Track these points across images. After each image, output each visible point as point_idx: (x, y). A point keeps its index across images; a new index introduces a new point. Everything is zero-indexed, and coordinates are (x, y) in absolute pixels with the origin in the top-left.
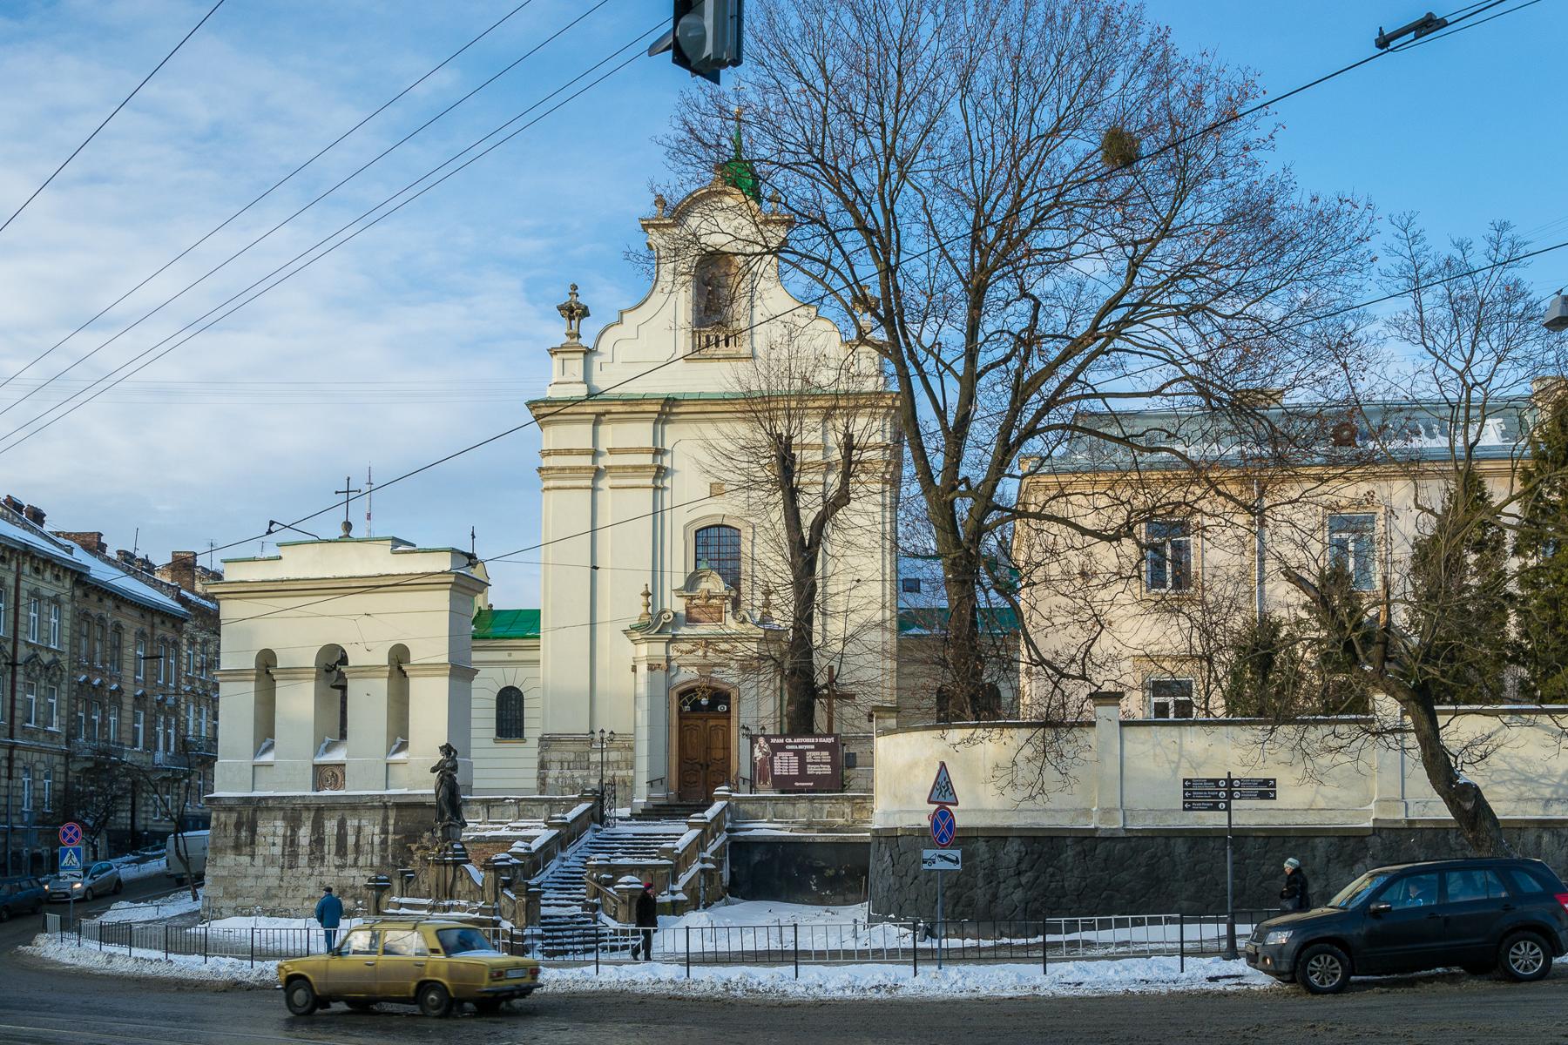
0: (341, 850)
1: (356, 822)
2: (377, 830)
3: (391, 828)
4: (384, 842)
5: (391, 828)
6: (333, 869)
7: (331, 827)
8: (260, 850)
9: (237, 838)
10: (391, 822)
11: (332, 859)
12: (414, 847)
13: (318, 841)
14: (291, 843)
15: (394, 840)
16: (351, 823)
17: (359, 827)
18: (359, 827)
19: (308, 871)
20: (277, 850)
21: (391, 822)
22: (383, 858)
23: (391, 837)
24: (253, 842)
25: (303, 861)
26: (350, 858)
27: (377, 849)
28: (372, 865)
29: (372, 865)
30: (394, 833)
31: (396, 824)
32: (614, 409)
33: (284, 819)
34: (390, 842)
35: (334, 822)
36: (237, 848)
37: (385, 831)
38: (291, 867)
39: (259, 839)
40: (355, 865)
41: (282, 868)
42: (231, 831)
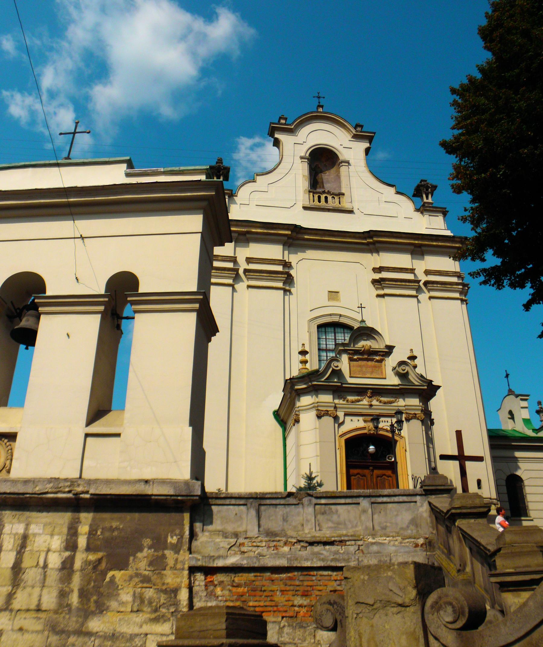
1: (20, 529)
2: (57, 542)
3: (82, 541)
5: (82, 541)
10: (84, 529)
12: (118, 575)
15: (87, 563)
17: (25, 537)
18: (25, 537)
21: (84, 529)
22: (63, 595)
23: (80, 558)
27: (53, 576)
28: (38, 610)
29: (38, 610)
30: (88, 549)
31: (91, 534)
34: (78, 565)
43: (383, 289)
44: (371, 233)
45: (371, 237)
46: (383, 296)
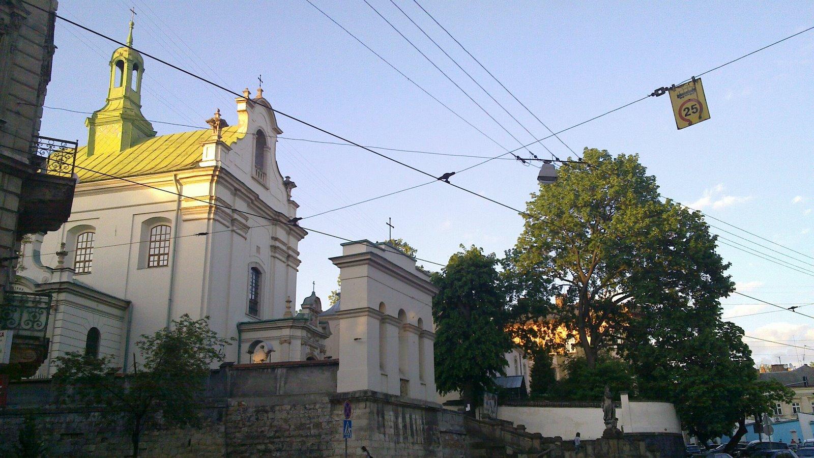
0: (412, 435)
4: (423, 428)
6: (411, 444)
7: (407, 416)
8: (387, 430)
9: (378, 422)
11: (410, 439)
13: (405, 426)
14: (396, 426)
16: (413, 416)
19: (403, 445)
20: (392, 431)
24: (384, 426)
25: (401, 439)
26: (415, 437)
32: (243, 190)
33: (393, 411)
35: (408, 415)
36: (378, 428)
37: (423, 423)
38: (398, 443)
39: (386, 423)
40: (417, 443)
41: (395, 442)
42: (376, 416)
43: (275, 252)
44: (281, 214)
45: (279, 216)
46: (274, 257)
